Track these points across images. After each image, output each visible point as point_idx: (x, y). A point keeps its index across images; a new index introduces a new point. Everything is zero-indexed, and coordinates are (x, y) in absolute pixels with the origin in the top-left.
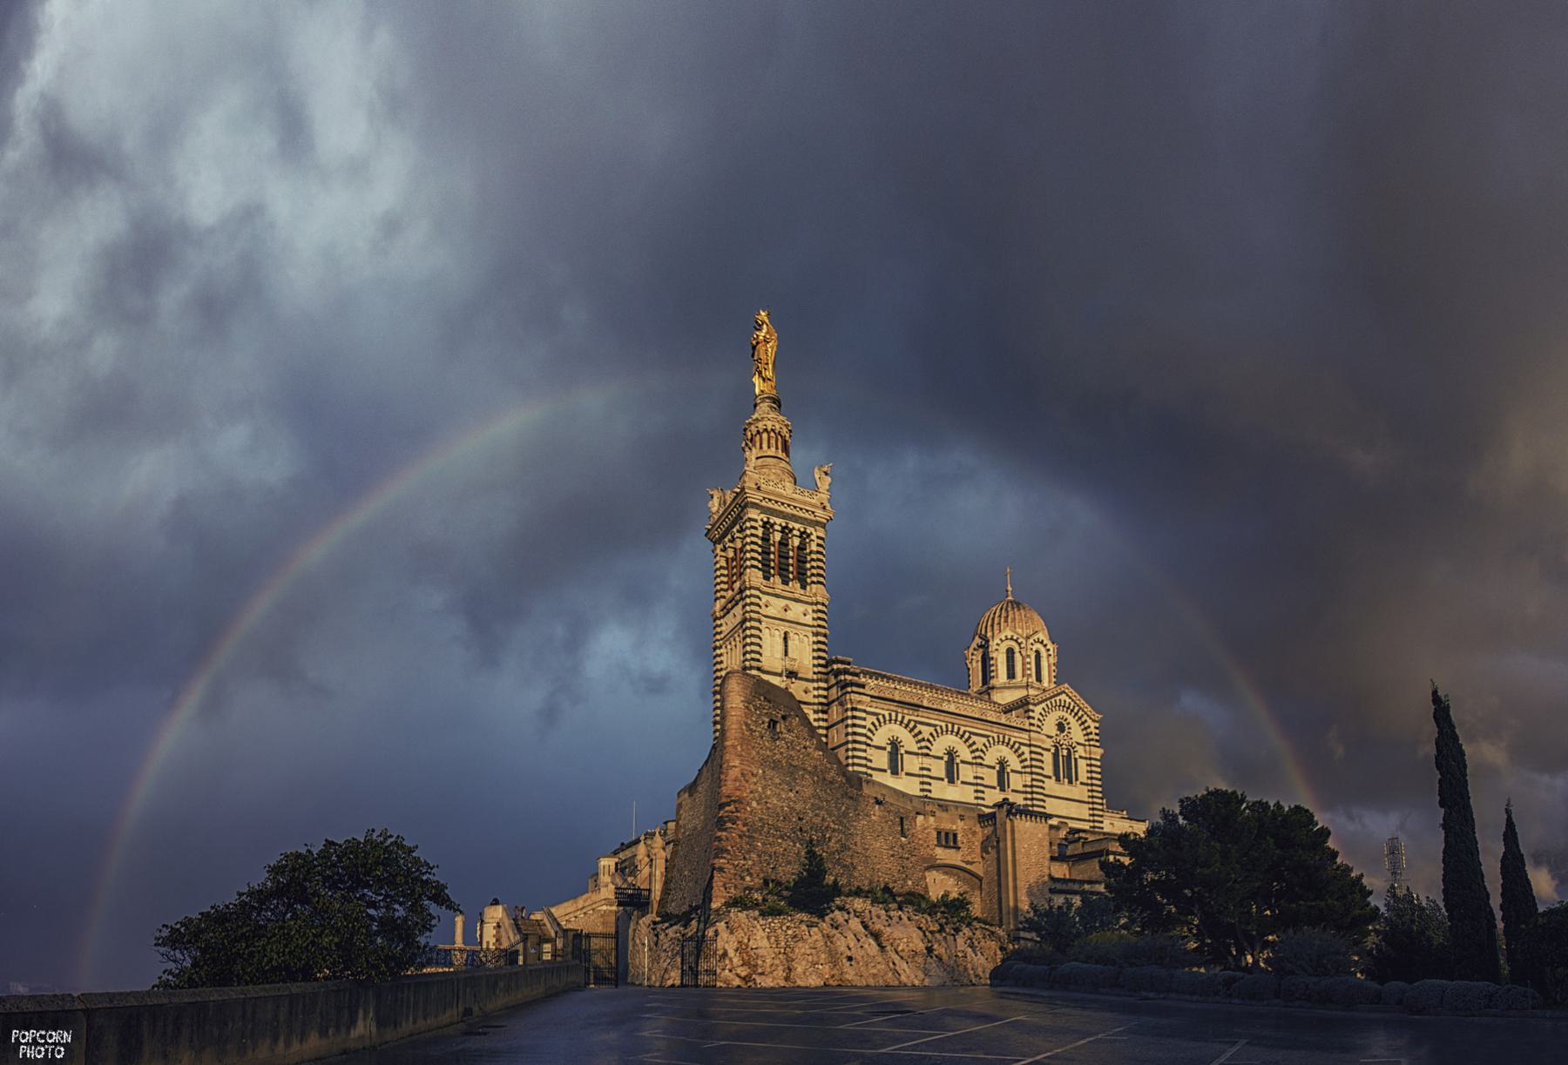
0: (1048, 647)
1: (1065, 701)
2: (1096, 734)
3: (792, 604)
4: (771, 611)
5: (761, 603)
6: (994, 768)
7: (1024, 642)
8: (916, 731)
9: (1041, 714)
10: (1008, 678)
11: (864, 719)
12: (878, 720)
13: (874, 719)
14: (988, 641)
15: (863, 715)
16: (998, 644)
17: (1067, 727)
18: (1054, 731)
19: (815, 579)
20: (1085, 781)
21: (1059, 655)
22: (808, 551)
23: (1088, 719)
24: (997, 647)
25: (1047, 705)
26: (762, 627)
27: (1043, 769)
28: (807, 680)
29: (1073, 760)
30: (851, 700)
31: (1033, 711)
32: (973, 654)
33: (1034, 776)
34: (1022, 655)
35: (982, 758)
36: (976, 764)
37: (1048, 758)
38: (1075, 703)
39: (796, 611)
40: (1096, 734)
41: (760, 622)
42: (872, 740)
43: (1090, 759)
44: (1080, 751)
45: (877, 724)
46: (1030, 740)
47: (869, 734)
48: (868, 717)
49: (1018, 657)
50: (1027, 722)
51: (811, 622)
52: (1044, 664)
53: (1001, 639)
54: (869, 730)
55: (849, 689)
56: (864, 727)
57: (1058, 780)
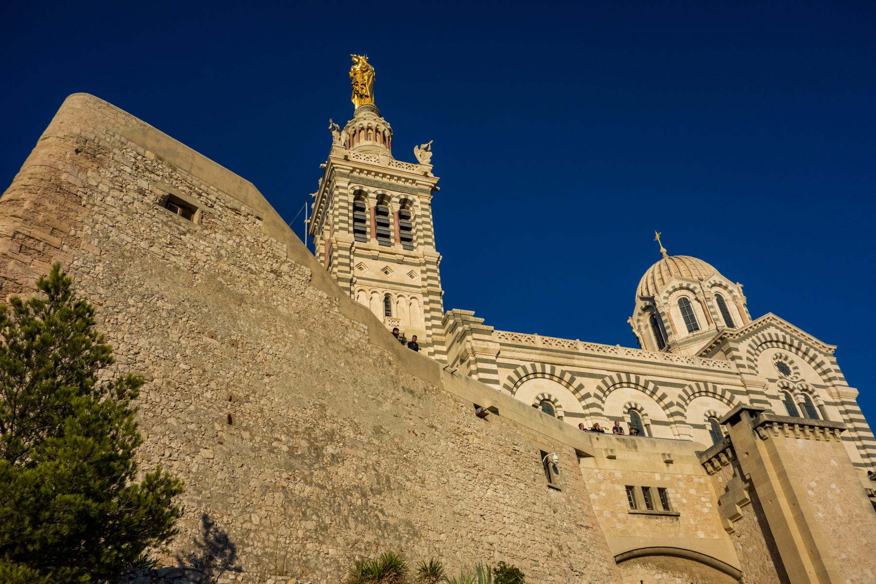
0: (730, 288)
2: (836, 371)
3: (393, 266)
6: (703, 427)
7: (698, 286)
8: (575, 384)
9: (748, 352)
10: (690, 331)
12: (517, 373)
13: (511, 372)
14: (652, 299)
15: (494, 367)
16: (665, 298)
17: (791, 367)
18: (776, 373)
19: (421, 241)
21: (746, 292)
22: (412, 218)
23: (817, 353)
24: (666, 301)
25: (753, 341)
29: (817, 409)
30: (472, 348)
31: (737, 350)
32: (638, 321)
34: (699, 301)
35: (682, 415)
36: (675, 422)
38: (791, 336)
39: (399, 273)
40: (836, 371)
43: (843, 403)
44: (823, 396)
46: (745, 386)
49: (695, 306)
50: (733, 365)
51: (420, 283)
52: (731, 307)
53: (667, 292)
54: (506, 386)
55: (469, 338)
56: (497, 382)
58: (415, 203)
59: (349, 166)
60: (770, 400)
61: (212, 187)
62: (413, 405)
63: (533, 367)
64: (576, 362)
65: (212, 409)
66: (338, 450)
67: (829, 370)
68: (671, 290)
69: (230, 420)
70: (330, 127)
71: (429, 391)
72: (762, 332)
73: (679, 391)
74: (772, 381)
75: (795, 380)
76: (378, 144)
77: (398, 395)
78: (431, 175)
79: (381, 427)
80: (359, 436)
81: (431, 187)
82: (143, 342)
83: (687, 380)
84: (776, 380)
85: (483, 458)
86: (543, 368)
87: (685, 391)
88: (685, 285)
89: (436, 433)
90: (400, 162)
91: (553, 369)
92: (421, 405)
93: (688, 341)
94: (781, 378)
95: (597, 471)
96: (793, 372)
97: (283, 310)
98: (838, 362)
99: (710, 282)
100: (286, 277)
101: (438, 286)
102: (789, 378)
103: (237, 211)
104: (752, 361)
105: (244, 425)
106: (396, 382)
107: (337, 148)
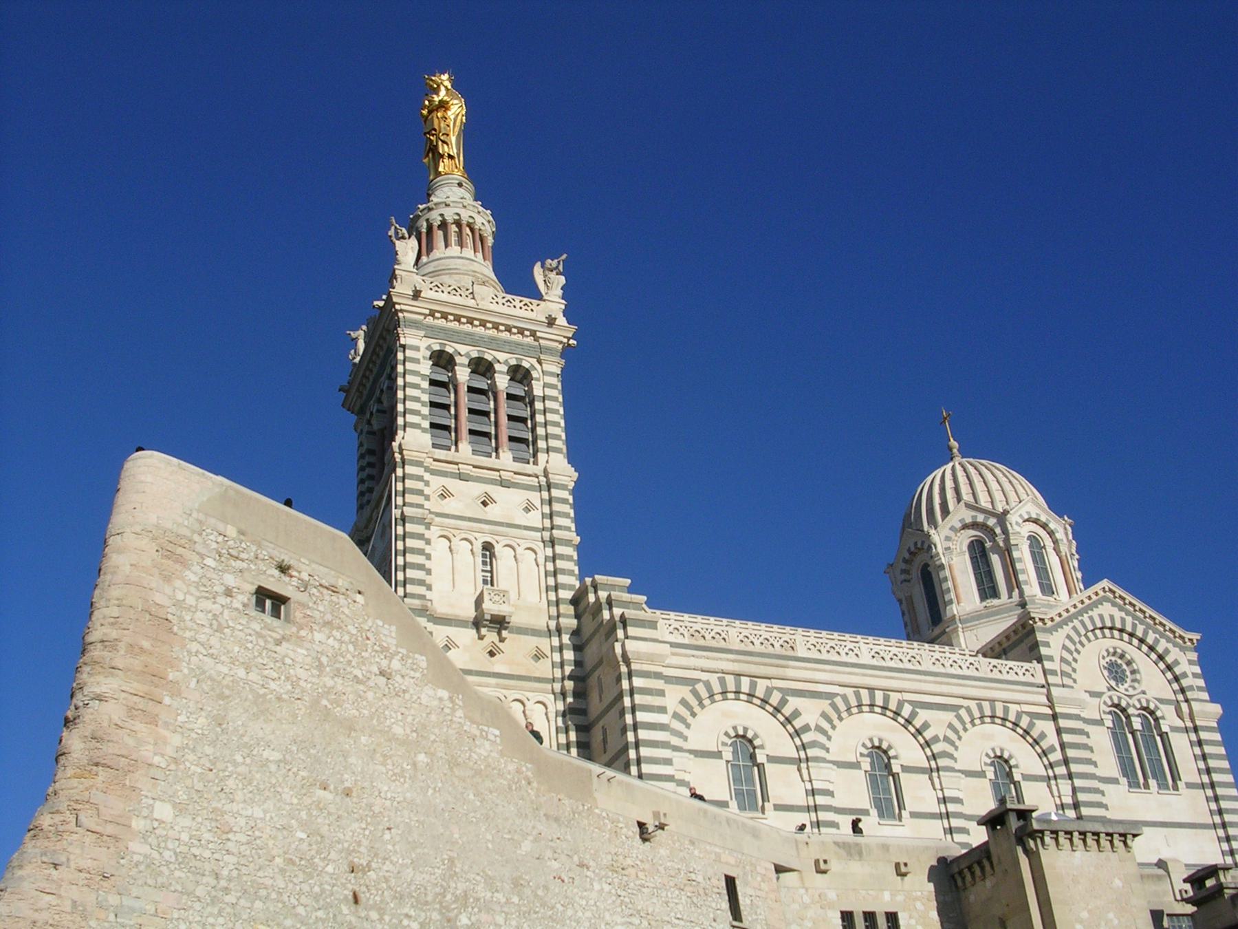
1: (1112, 618)
2: (1195, 675)
3: (496, 492)
4: (449, 506)
5: (427, 491)
6: (982, 774)
9: (1064, 647)
11: (661, 693)
13: (685, 692)
15: (658, 684)
20: (1196, 779)
21: (1078, 534)
23: (1170, 646)
25: (1074, 628)
26: (432, 534)
27: (1095, 764)
28: (535, 632)
33: (1078, 783)
35: (951, 756)
37: (1101, 739)
39: (508, 504)
40: (1195, 675)
41: (428, 526)
42: (685, 739)
45: (693, 702)
47: (676, 725)
48: (669, 689)
52: (1053, 560)
53: (952, 528)
54: (676, 716)
56: (662, 710)
57: (1133, 784)
58: (534, 374)
59: (422, 307)
60: (1088, 728)
61: (302, 560)
62: (558, 839)
63: (722, 682)
64: (790, 673)
65: (335, 888)
66: (473, 918)
67: (1185, 675)
68: (959, 525)
69: (356, 900)
70: (392, 232)
71: (579, 814)
72: (1090, 613)
73: (949, 716)
74: (1093, 694)
75: (1131, 692)
76: (468, 252)
77: (540, 827)
78: (562, 321)
79: (521, 877)
80: (496, 894)
81: (561, 342)
82: (258, 812)
83: (964, 698)
84: (1104, 693)
85: (647, 900)
86: (738, 684)
87: (959, 718)
88: (981, 518)
89: (589, 874)
90: (509, 297)
91: (753, 685)
92: (569, 837)
93: (976, 617)
94: (1111, 688)
95: (802, 891)
96: (1130, 677)
97: (398, 730)
98: (1201, 662)
99: (1021, 516)
100: (398, 678)
101: (568, 529)
102: (1122, 688)
103: (333, 590)
104: (1068, 663)
105: (371, 902)
106: (537, 809)
107: (403, 274)
